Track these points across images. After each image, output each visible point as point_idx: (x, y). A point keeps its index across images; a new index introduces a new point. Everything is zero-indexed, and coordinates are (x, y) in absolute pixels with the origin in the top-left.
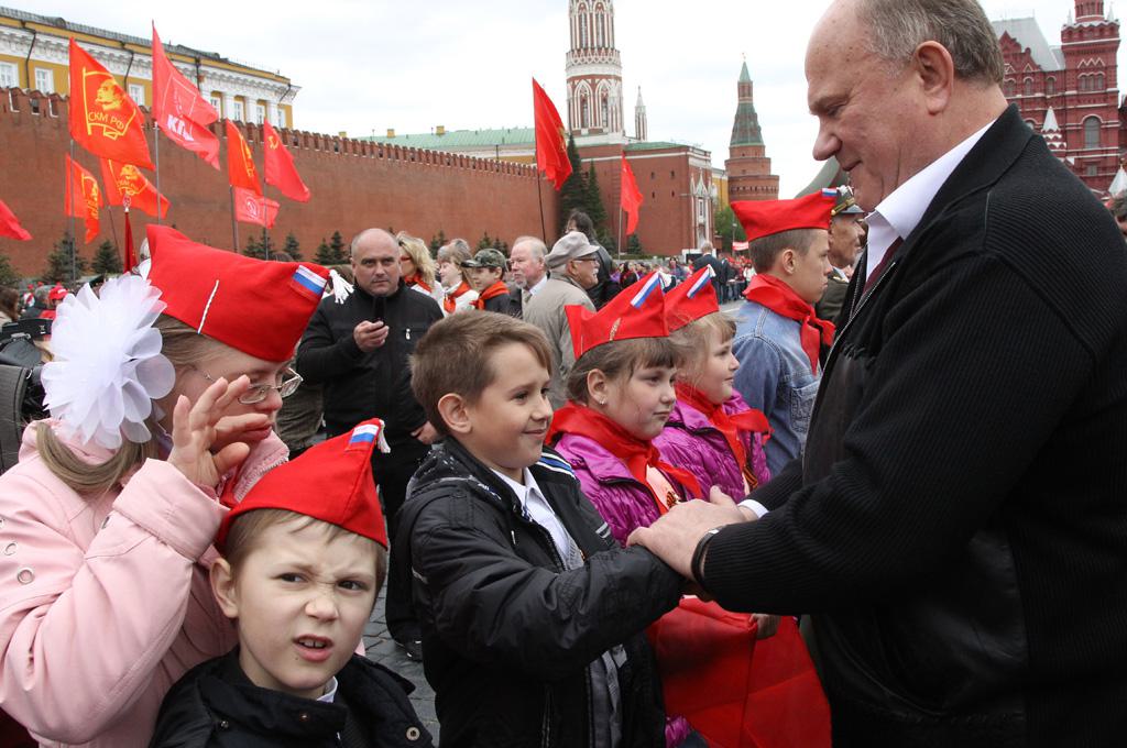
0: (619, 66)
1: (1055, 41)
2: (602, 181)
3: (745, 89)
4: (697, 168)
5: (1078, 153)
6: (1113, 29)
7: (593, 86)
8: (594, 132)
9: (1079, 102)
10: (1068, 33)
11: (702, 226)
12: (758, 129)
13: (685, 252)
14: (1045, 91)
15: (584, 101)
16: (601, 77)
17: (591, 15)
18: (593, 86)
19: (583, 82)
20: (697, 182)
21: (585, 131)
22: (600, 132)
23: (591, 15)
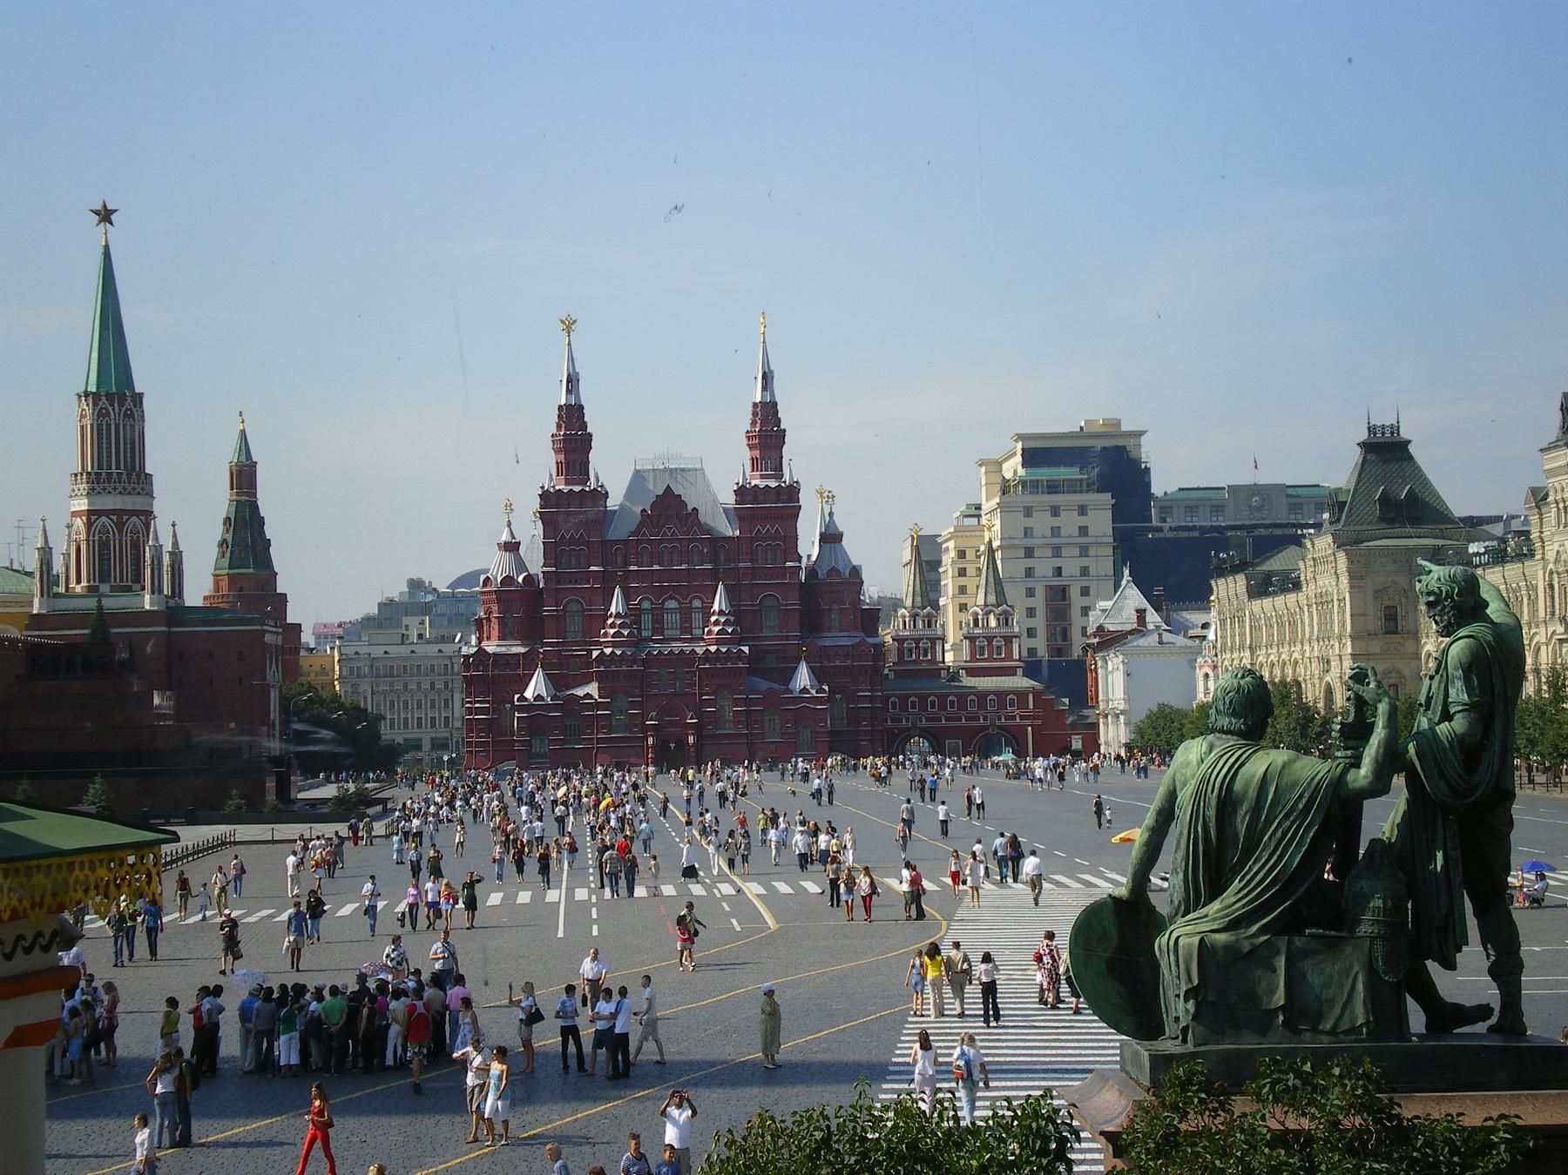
0: (150, 495)
1: (729, 499)
3: (244, 477)
5: (754, 639)
6: (792, 492)
7: (120, 525)
8: (113, 589)
9: (754, 577)
10: (741, 492)
12: (267, 543)
14: (714, 561)
16: (131, 513)
17: (117, 426)
18: (120, 525)
21: (105, 588)
23: (117, 426)
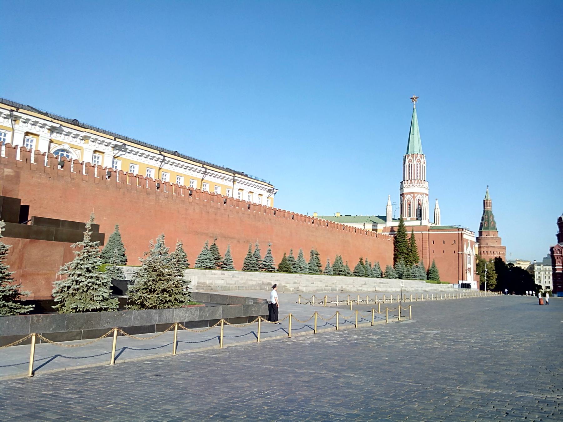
2: (418, 243)
4: (468, 240)
7: (414, 197)
8: (412, 220)
11: (470, 269)
12: (495, 223)
13: (461, 282)
15: (410, 205)
16: (418, 193)
17: (414, 165)
18: (414, 197)
19: (409, 196)
20: (467, 248)
21: (409, 219)
22: (417, 219)
23: (414, 165)
